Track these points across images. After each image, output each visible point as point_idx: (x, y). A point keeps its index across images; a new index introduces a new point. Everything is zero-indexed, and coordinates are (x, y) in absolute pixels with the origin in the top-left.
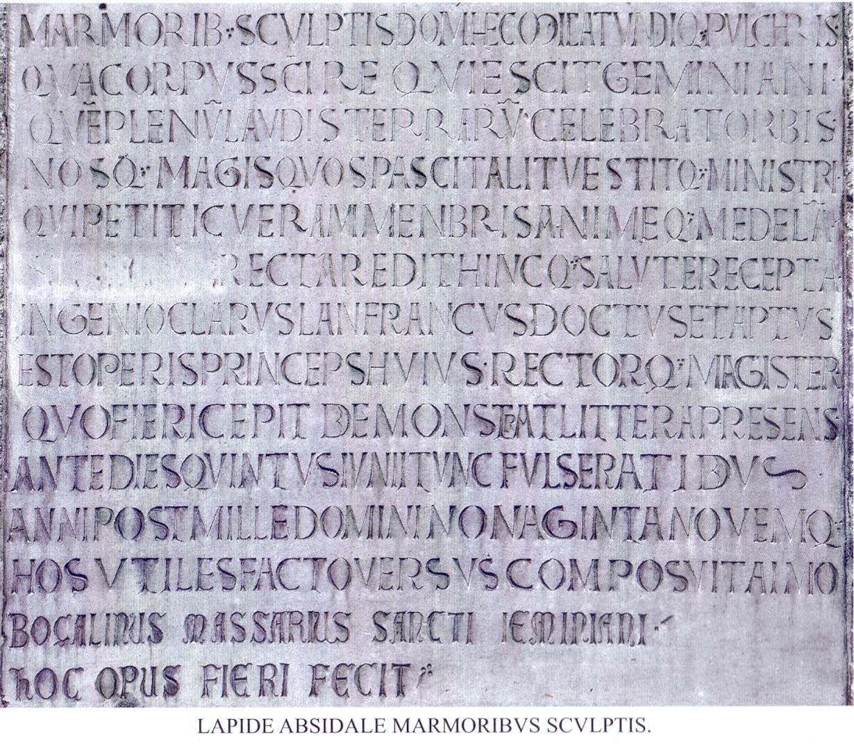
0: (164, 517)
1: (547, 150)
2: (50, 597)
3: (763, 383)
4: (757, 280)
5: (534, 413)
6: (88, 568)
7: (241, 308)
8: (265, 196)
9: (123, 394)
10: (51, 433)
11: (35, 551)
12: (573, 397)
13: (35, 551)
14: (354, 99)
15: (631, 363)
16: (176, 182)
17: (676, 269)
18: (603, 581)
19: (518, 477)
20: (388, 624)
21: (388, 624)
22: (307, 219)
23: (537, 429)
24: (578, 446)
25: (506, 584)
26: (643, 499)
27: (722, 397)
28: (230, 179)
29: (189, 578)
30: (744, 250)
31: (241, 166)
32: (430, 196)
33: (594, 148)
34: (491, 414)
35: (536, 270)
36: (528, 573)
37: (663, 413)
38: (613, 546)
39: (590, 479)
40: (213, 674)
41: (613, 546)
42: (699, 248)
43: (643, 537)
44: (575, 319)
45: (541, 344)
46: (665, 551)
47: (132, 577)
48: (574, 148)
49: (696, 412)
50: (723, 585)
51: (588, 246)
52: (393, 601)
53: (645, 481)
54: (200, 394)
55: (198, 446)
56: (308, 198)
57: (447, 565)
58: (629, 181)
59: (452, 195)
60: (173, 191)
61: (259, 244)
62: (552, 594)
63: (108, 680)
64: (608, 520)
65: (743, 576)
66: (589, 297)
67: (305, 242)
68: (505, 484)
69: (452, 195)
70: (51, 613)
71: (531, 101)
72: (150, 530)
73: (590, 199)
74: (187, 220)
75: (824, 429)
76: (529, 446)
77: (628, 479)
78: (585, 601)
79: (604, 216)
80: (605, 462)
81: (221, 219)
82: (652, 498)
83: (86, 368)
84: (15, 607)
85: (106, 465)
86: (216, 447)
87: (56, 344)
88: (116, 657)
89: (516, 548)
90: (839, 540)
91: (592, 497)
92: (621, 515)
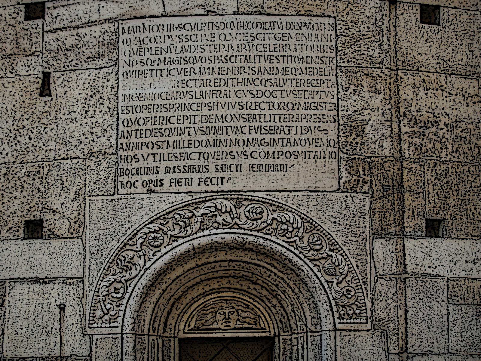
0: (159, 143)
1: (260, 54)
2: (129, 164)
3: (317, 109)
4: (315, 84)
5: (258, 117)
6: (139, 156)
7: (179, 94)
8: (186, 66)
9: (148, 115)
10: (130, 125)
11: (125, 153)
12: (268, 112)
13: (125, 153)
14: (209, 43)
15: (283, 104)
16: (163, 63)
17: (294, 82)
18: (276, 156)
19: (253, 132)
20: (219, 168)
21: (219, 168)
22: (197, 71)
23: (258, 120)
24: (269, 124)
25: (250, 157)
26: (286, 137)
27: (306, 112)
28: (176, 62)
29: (166, 158)
30: (311, 78)
31: (179, 59)
32: (230, 65)
33: (272, 54)
34: (247, 117)
35: (257, 82)
36: (256, 155)
37: (291, 116)
38: (279, 148)
39: (272, 132)
40: (172, 181)
41: (279, 148)
42: (300, 77)
43: (287, 145)
44: (268, 94)
45: (259, 100)
46: (292, 149)
47: (151, 158)
48: (267, 54)
49: (300, 116)
50: (307, 157)
51: (271, 77)
52: (220, 162)
53: (287, 132)
54: (169, 114)
55: (169, 126)
56: (197, 66)
57: (234, 153)
58: (281, 61)
59: (234, 65)
60: (162, 66)
61: (184, 78)
62: (262, 160)
63: (145, 183)
64: (277, 141)
65: (312, 155)
66: (271, 88)
67: (196, 77)
68: (250, 133)
69: (234, 65)
70: (130, 168)
71: (255, 42)
72: (156, 147)
73: (271, 65)
74: (164, 73)
75: (333, 120)
76: (257, 124)
77: (282, 132)
78: (270, 161)
79: (275, 69)
80: (276, 128)
81: (174, 72)
82: (289, 136)
83: (138, 109)
84: (120, 166)
85: (144, 132)
86: (173, 127)
87: (131, 103)
88: (147, 178)
89: (253, 149)
90: (337, 146)
91: (272, 136)
92: (280, 141)
